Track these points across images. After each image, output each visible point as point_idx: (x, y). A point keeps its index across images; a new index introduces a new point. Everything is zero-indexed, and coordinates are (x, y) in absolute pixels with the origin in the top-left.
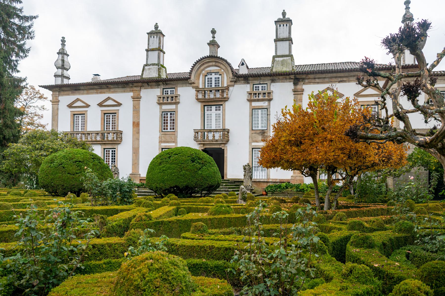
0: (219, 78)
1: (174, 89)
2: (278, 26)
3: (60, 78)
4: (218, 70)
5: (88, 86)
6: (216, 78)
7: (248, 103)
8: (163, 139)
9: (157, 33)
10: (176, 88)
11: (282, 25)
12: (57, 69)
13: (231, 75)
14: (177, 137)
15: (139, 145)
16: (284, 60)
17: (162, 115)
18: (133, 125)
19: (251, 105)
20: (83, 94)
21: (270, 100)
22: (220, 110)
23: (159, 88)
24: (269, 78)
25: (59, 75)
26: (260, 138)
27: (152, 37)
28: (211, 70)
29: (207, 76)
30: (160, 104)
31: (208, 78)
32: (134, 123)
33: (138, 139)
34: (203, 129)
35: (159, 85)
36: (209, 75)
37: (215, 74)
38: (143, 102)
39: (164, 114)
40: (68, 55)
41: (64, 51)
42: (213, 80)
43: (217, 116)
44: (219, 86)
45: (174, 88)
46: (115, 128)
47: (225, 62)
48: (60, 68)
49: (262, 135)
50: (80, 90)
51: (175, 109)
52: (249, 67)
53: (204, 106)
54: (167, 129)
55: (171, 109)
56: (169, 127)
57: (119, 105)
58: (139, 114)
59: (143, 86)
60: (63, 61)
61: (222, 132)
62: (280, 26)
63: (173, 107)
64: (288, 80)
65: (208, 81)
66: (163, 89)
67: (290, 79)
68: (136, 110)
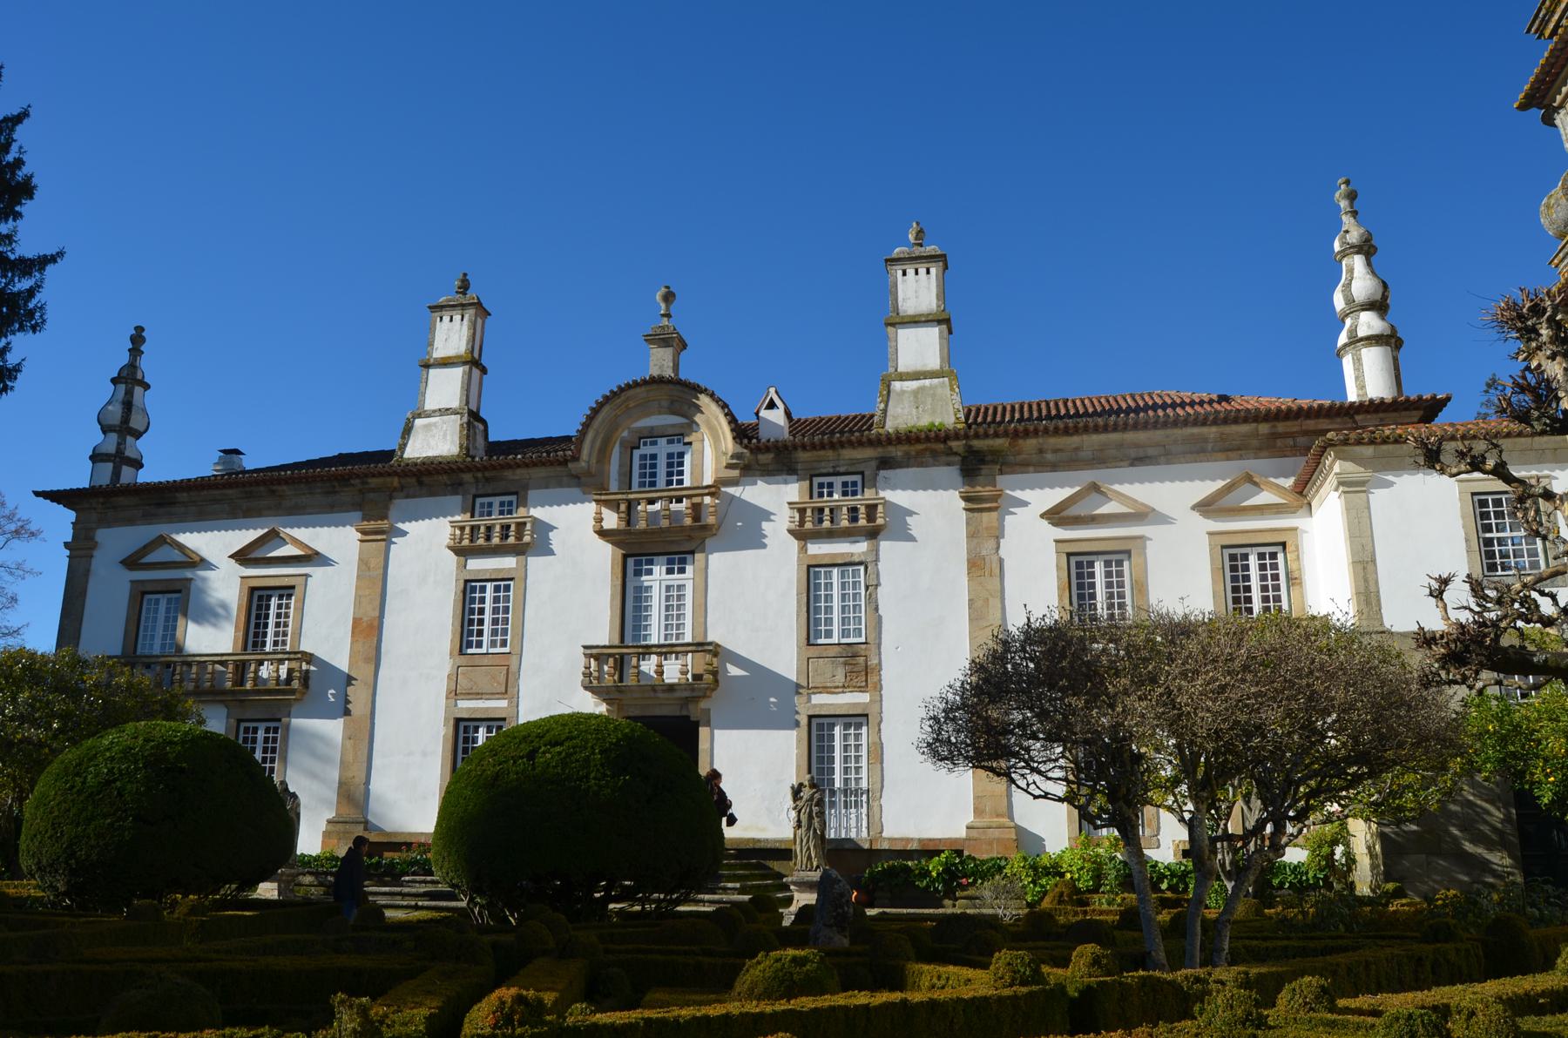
2: (900, 273)
3: (110, 466)
4: (681, 425)
6: (670, 456)
7: (794, 544)
11: (911, 272)
12: (104, 432)
16: (922, 389)
17: (464, 592)
18: (353, 633)
19: (803, 549)
23: (457, 494)
25: (107, 455)
27: (446, 319)
28: (652, 428)
29: (638, 448)
30: (462, 552)
31: (643, 457)
34: (616, 642)
35: (461, 484)
36: (645, 444)
39: (469, 590)
40: (147, 387)
41: (135, 373)
42: (662, 463)
43: (674, 597)
45: (516, 493)
46: (284, 643)
48: (115, 431)
49: (845, 664)
50: (173, 504)
52: (795, 417)
53: (625, 557)
54: (479, 644)
59: (402, 488)
60: (128, 405)
61: (690, 655)
62: (904, 274)
63: (508, 563)
64: (944, 459)
65: (643, 466)
66: (475, 497)
67: (948, 455)
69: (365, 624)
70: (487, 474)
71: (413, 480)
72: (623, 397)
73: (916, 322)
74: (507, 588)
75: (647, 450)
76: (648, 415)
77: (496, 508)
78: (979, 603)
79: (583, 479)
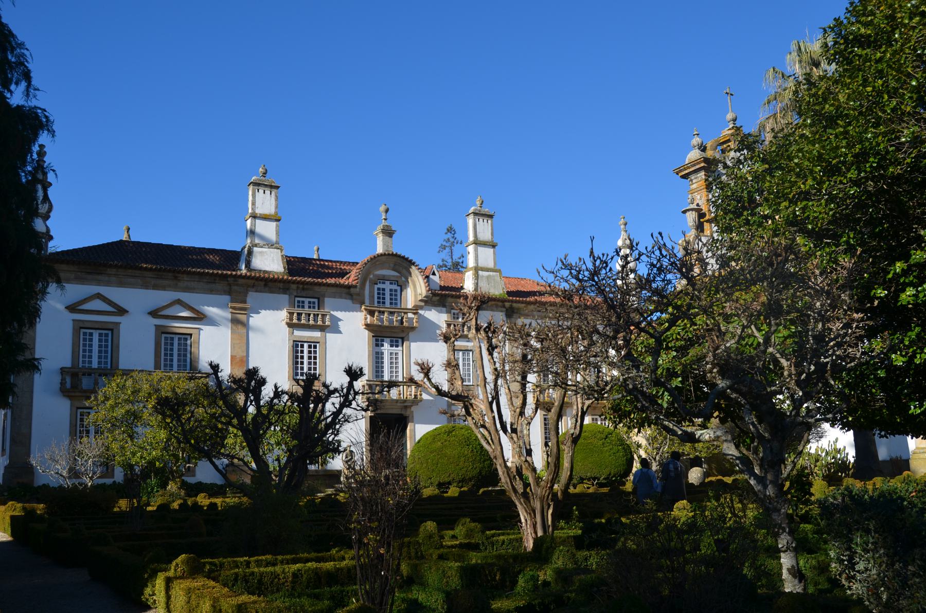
1: (316, 300)
4: (397, 276)
5: (130, 271)
6: (391, 290)
10: (321, 299)
20: (108, 284)
27: (261, 191)
28: (384, 276)
30: (290, 325)
31: (379, 289)
35: (288, 289)
37: (391, 284)
39: (297, 346)
59: (253, 286)
63: (317, 334)
64: (500, 309)
65: (379, 294)
66: (296, 296)
74: (315, 347)
75: (381, 286)
76: (382, 269)
77: (306, 305)
79: (354, 297)
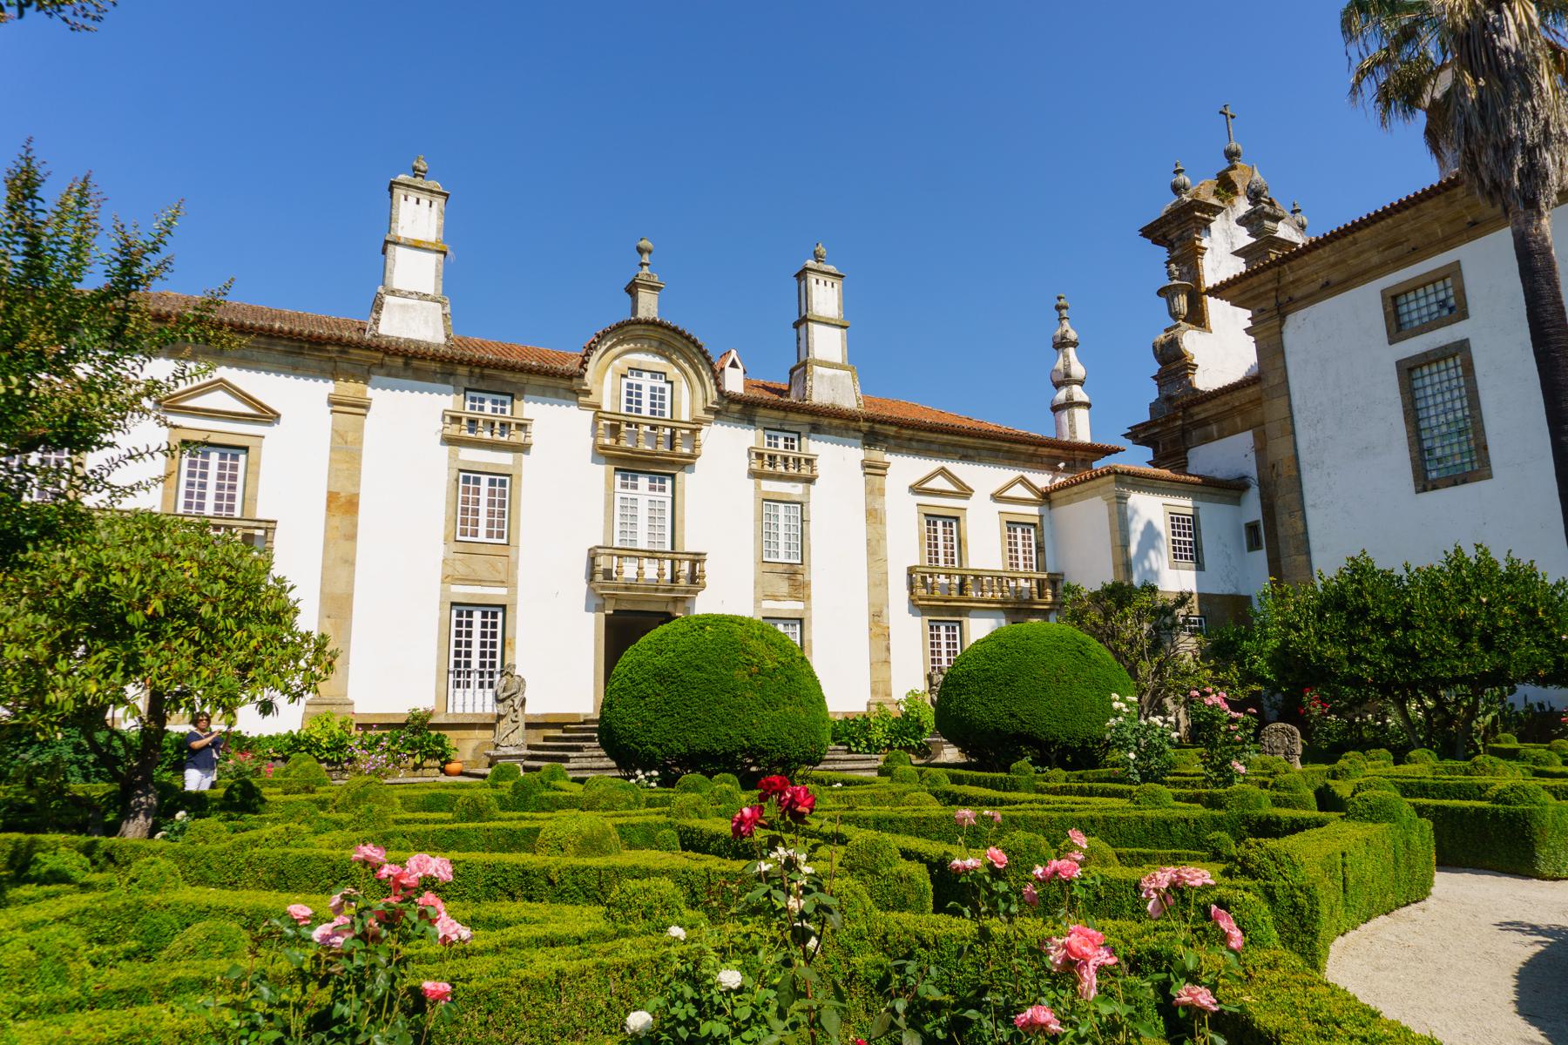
0: (662, 390)
2: (814, 281)
6: (653, 389)
8: (461, 570)
9: (431, 191)
13: (713, 394)
14: (516, 563)
15: (351, 583)
18: (328, 506)
19: (758, 486)
21: (810, 480)
22: (663, 489)
23: (448, 383)
24: (807, 418)
26: (783, 587)
27: (412, 199)
31: (630, 386)
32: (332, 497)
33: (350, 562)
35: (451, 374)
37: (653, 377)
38: (372, 423)
44: (662, 413)
46: (231, 508)
47: (695, 350)
49: (789, 579)
51: (514, 466)
54: (475, 534)
55: (498, 465)
56: (483, 528)
57: (266, 415)
58: (360, 464)
59: (382, 365)
62: (817, 282)
63: (504, 459)
64: (852, 433)
65: (630, 394)
68: (346, 452)
69: (343, 500)
70: (487, 371)
71: (400, 361)
72: (626, 329)
73: (827, 324)
75: (634, 380)
78: (874, 543)
